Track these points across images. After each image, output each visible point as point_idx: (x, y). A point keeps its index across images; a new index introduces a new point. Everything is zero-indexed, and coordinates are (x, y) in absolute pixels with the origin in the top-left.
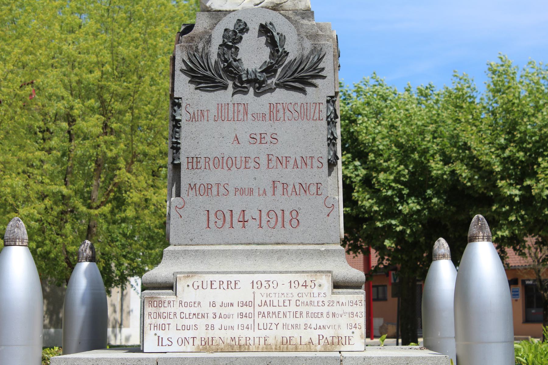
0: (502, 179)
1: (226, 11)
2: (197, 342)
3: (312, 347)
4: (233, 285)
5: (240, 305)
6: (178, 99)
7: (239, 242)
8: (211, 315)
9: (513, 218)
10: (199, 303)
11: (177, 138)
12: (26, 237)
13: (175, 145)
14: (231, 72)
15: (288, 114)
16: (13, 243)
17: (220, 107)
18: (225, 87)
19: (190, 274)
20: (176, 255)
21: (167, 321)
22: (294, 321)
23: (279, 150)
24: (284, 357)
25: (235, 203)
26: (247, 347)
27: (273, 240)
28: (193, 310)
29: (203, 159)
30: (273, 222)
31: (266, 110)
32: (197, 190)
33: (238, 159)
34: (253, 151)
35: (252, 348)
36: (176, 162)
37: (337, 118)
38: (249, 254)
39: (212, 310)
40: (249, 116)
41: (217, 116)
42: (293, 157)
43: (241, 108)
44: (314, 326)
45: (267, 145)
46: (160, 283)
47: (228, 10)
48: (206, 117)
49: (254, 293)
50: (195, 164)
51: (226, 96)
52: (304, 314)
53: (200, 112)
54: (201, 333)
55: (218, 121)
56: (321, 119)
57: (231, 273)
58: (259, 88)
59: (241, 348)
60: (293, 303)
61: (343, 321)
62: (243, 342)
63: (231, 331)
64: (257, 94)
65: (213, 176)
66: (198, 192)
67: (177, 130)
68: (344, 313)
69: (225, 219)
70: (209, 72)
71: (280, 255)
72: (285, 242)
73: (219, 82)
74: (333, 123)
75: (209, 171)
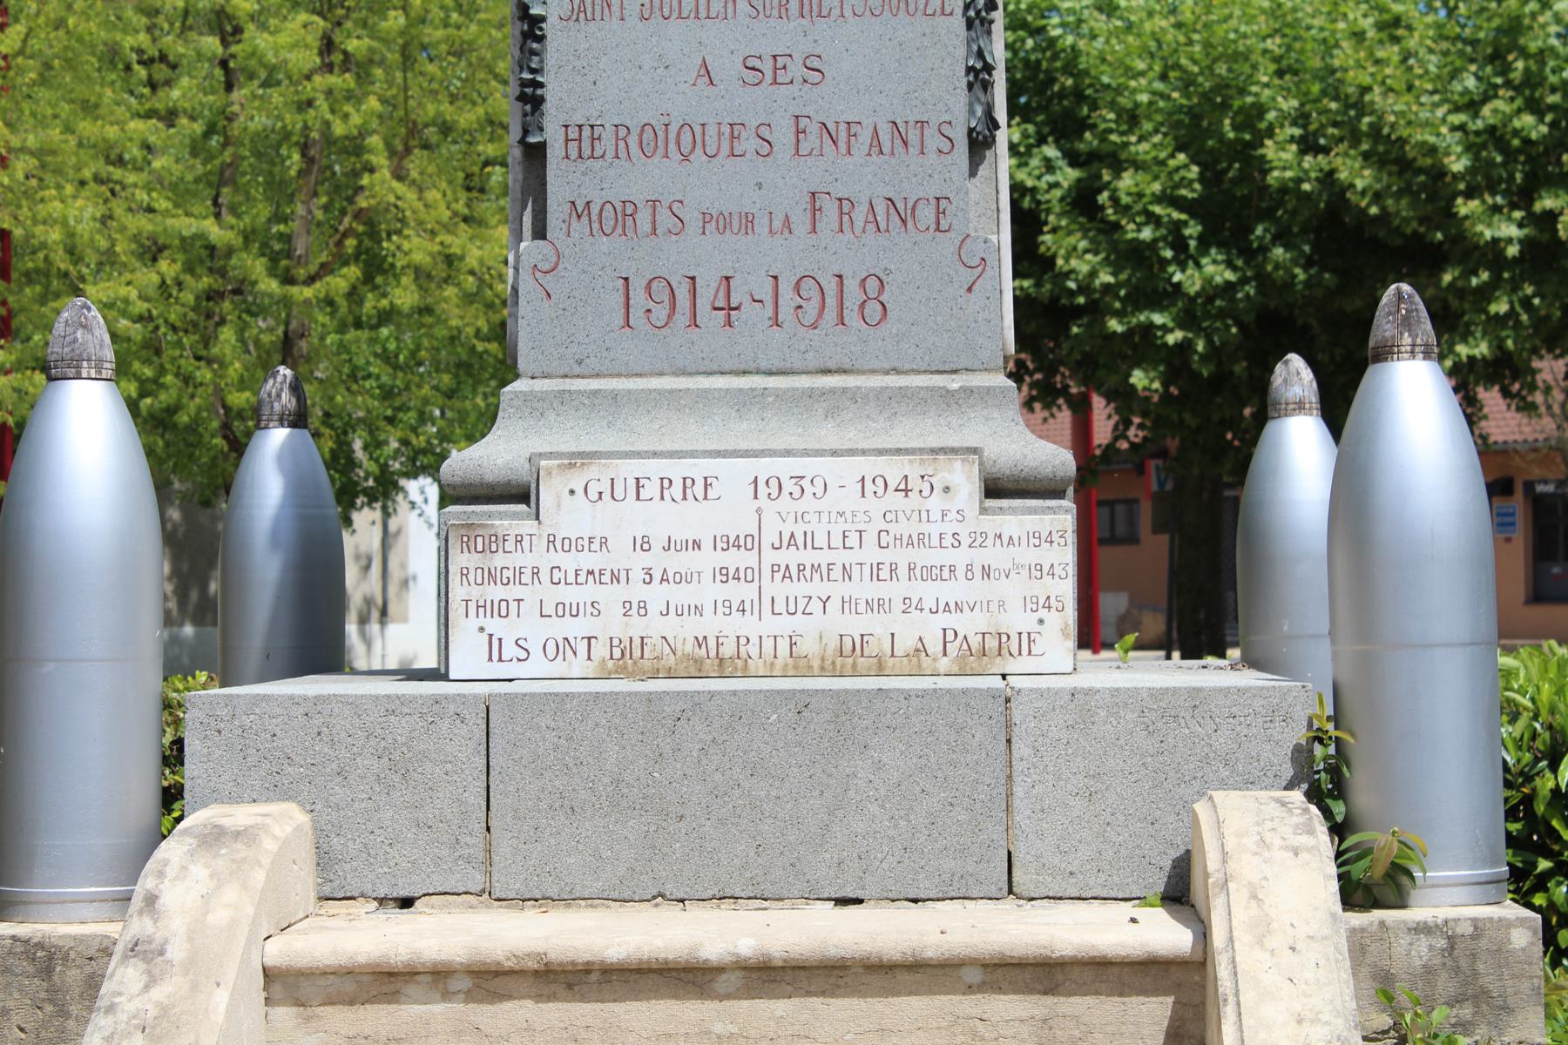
0: (1469, 194)
2: (600, 650)
4: (699, 490)
7: (716, 368)
8: (638, 575)
9: (1500, 307)
10: (604, 542)
11: (533, 71)
12: (109, 354)
13: (529, 90)
16: (71, 372)
19: (577, 460)
20: (536, 405)
21: (514, 591)
22: (873, 590)
23: (831, 104)
24: (846, 691)
25: (703, 256)
26: (740, 663)
27: (812, 361)
28: (588, 561)
29: (610, 128)
30: (811, 309)
32: (594, 217)
33: (711, 131)
34: (753, 104)
35: (756, 665)
36: (532, 140)
37: (995, 8)
38: (743, 402)
39: (639, 561)
41: (647, 5)
42: (868, 123)
44: (929, 603)
45: (794, 89)
46: (491, 486)
48: (615, 8)
50: (586, 144)
52: (903, 571)
54: (613, 625)
55: (653, 21)
56: (948, 11)
57: (692, 454)
59: (723, 667)
60: (870, 538)
61: (1013, 589)
62: (728, 650)
66: (596, 226)
67: (535, 45)
68: (1017, 566)
69: (676, 301)
71: (834, 403)
72: (847, 366)
74: (982, 24)
75: (627, 165)
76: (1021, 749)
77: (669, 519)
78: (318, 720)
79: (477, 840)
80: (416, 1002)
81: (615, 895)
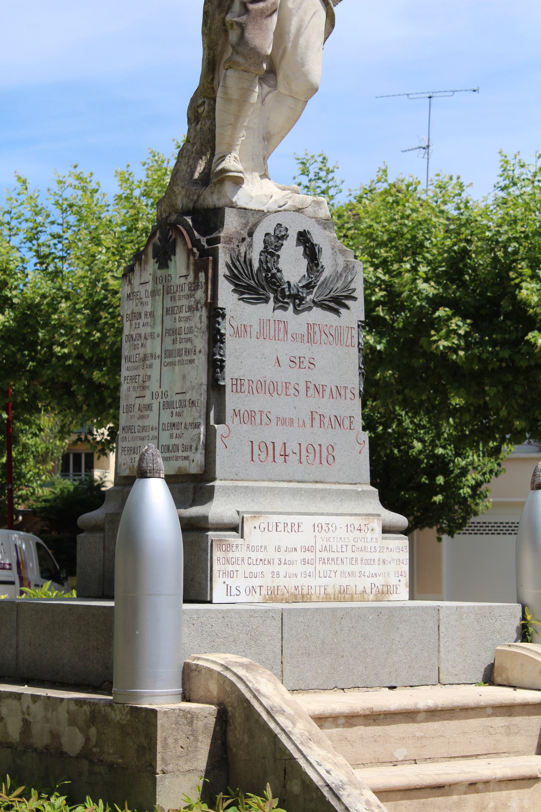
1: (255, 210)
2: (264, 592)
3: (366, 596)
4: (296, 528)
5: (303, 550)
6: (221, 309)
7: (281, 479)
8: (277, 561)
14: (274, 284)
15: (324, 336)
16: (157, 475)
17: (262, 323)
18: (266, 301)
19: (257, 514)
21: (236, 567)
23: (318, 377)
24: (392, 607)
25: (275, 434)
26: (309, 596)
27: (312, 477)
31: (304, 330)
32: (242, 416)
33: (280, 385)
35: (314, 598)
39: (277, 556)
40: (289, 336)
43: (282, 326)
44: (367, 574)
46: (225, 524)
47: (253, 208)
48: (248, 333)
49: (315, 536)
51: (266, 310)
52: (359, 561)
53: (243, 326)
54: (268, 582)
58: (299, 305)
60: (349, 548)
61: (392, 568)
62: (305, 591)
63: (295, 578)
64: (297, 311)
65: (257, 402)
66: (242, 420)
68: (393, 560)
69: (271, 452)
70: (252, 281)
71: (324, 495)
72: (323, 480)
73: (263, 295)
76: (442, 629)
77: (287, 539)
78: (227, 620)
79: (279, 667)
80: (328, 729)
81: (322, 688)
